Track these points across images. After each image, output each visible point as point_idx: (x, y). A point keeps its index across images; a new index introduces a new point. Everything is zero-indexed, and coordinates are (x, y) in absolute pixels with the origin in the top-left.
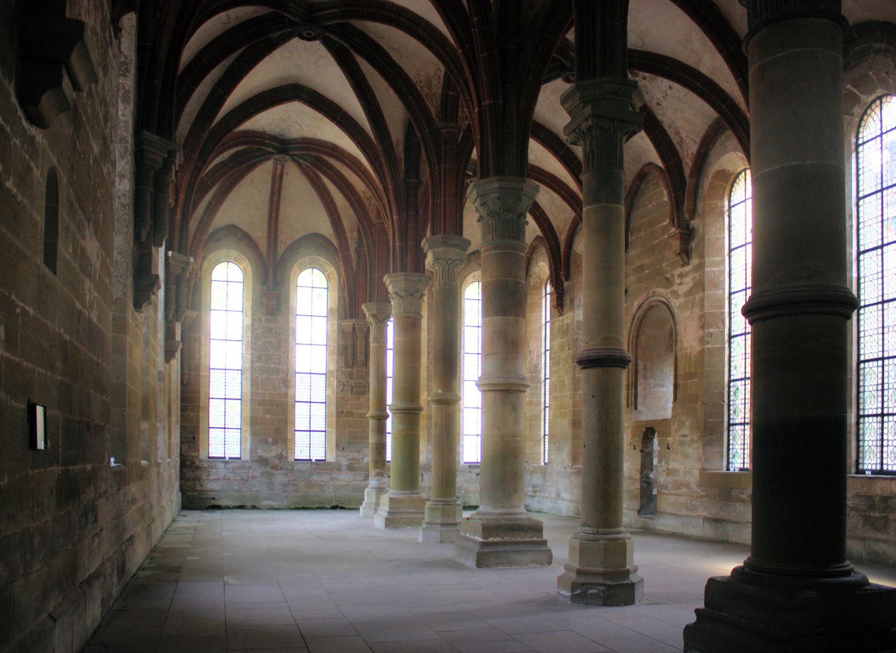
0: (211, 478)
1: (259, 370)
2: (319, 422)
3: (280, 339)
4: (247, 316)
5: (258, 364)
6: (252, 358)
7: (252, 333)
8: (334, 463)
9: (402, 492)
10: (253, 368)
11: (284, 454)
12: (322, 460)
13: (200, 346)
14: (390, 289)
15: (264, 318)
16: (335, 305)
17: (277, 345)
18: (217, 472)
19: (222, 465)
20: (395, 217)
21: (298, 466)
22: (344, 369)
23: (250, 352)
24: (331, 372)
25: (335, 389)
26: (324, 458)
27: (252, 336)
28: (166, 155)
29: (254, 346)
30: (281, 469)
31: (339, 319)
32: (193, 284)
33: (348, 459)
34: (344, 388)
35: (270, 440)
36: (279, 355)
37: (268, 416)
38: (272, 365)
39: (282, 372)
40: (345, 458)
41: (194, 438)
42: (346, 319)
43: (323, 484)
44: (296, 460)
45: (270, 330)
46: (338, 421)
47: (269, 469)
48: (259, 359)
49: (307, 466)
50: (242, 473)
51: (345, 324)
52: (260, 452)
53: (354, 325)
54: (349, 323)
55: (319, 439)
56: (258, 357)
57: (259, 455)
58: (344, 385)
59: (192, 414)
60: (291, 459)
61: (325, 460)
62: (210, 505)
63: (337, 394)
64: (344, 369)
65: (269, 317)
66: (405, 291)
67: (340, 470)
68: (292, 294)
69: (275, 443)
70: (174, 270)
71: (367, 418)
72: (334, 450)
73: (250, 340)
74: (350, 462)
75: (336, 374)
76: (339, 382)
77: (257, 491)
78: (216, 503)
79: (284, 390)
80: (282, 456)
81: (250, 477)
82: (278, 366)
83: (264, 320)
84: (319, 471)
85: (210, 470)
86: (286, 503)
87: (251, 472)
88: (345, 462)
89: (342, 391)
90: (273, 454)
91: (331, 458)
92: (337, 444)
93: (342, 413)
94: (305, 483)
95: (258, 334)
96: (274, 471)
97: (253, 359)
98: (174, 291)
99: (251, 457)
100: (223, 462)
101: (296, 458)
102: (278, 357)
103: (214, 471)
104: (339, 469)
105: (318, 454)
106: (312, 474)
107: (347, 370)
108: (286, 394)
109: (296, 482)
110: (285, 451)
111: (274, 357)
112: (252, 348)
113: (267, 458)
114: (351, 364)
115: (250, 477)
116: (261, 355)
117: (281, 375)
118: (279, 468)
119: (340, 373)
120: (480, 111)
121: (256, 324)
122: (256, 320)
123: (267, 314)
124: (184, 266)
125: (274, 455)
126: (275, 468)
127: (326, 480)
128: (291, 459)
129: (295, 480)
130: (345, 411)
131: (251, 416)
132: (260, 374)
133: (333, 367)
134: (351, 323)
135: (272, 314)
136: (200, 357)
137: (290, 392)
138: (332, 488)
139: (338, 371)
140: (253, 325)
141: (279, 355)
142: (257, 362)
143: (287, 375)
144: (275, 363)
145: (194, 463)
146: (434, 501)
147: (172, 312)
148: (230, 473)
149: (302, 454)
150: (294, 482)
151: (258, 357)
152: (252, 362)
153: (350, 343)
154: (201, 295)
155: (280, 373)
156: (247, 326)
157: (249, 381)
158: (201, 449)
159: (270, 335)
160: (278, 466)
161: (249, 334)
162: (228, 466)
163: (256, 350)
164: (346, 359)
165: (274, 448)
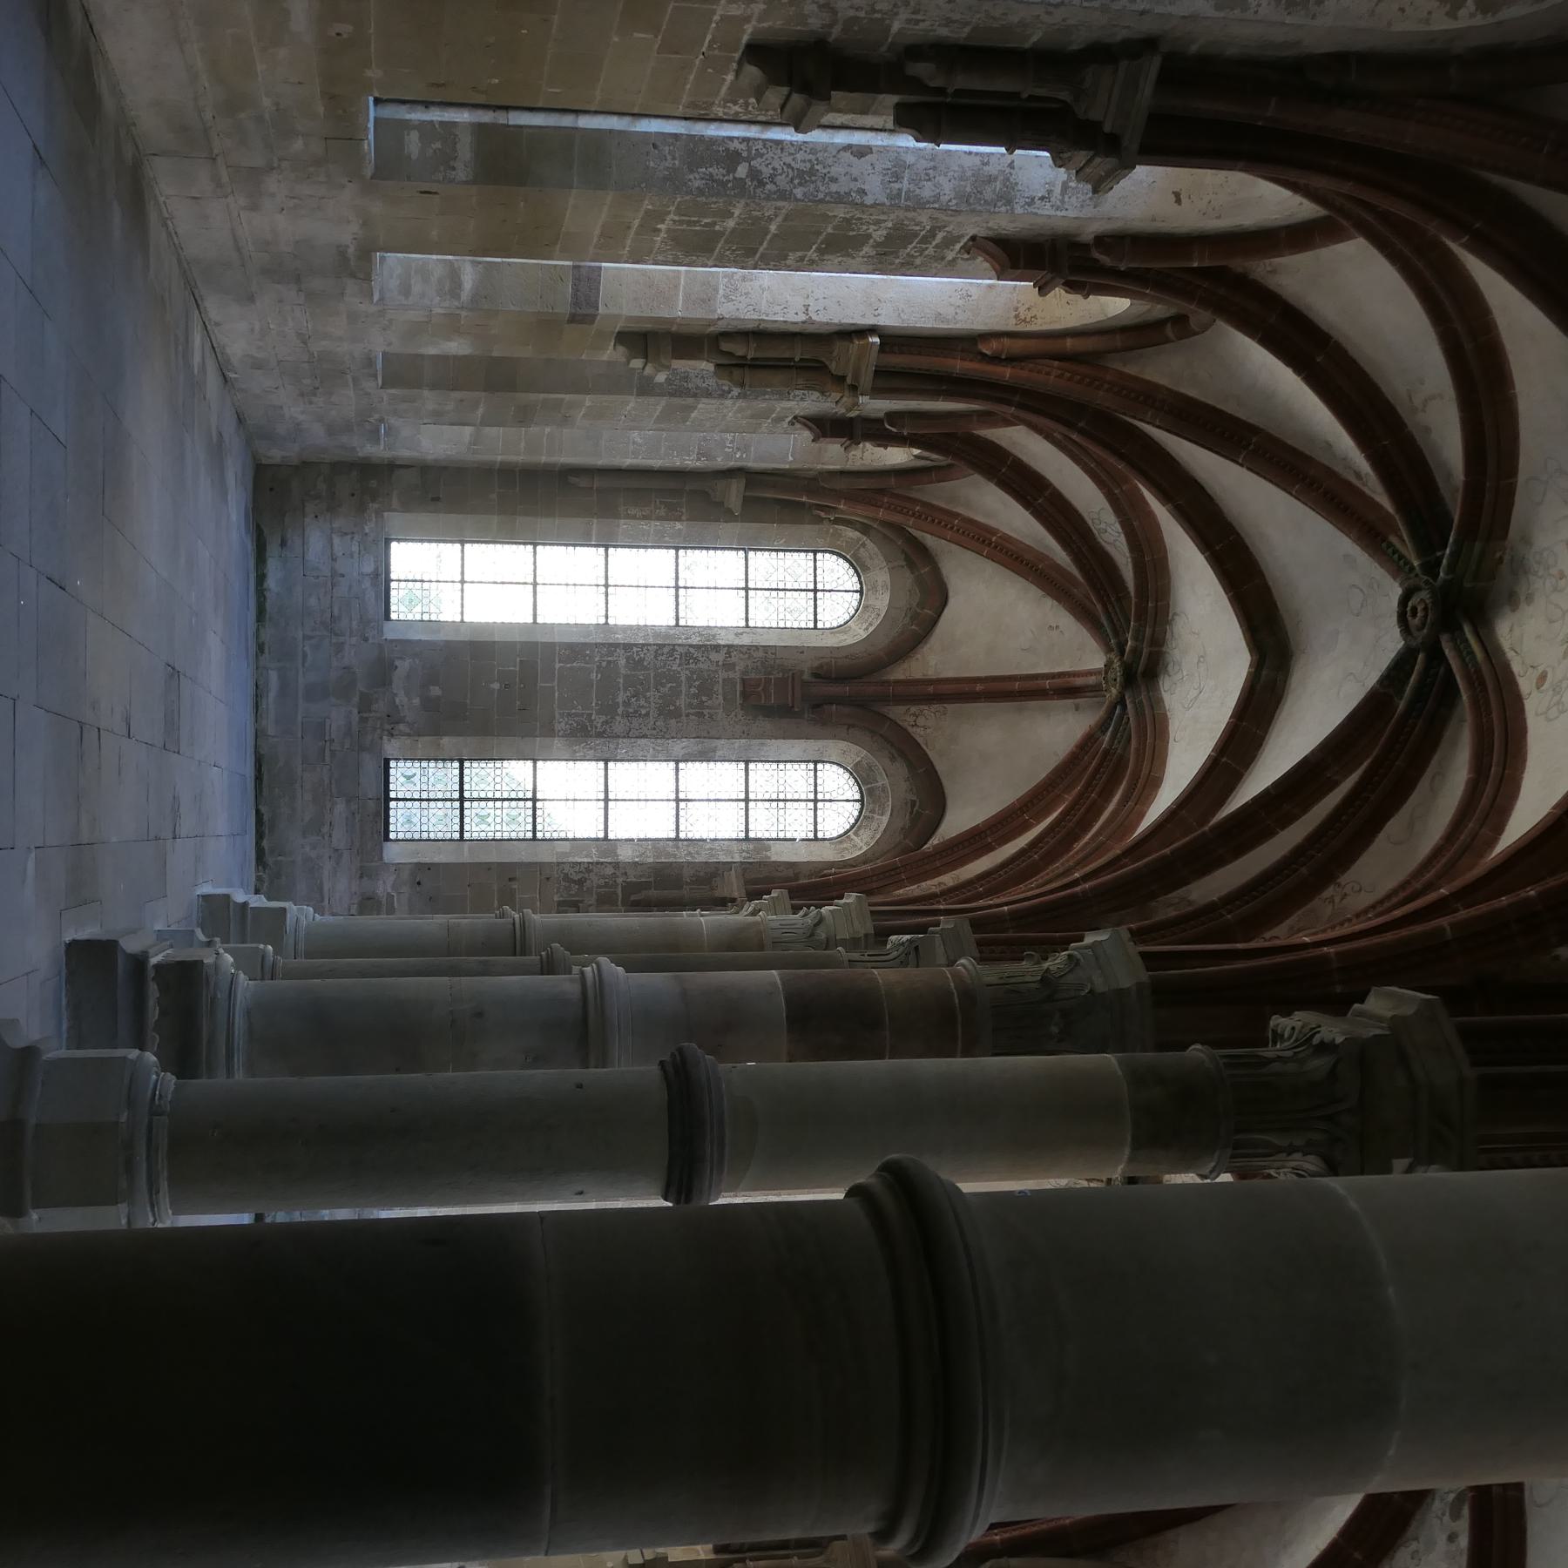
0: (336, 540)
1: (609, 662)
2: (487, 823)
3: (687, 715)
4: (737, 635)
5: (622, 662)
6: (636, 645)
7: (697, 647)
8: (381, 858)
9: (302, 934)
10: (613, 647)
11: (402, 727)
12: (387, 831)
13: (658, 518)
14: (825, 910)
15: (735, 675)
16: (779, 855)
17: (672, 708)
18: (352, 556)
19: (368, 568)
20: (1006, 908)
21: (370, 765)
22: (620, 880)
23: (651, 641)
24: (614, 852)
25: (571, 859)
26: (392, 836)
27: (691, 646)
28: (1107, 128)
29: (666, 650)
30: (363, 720)
31: (745, 867)
32: (804, 499)
33: (390, 897)
34: (574, 882)
35: (435, 691)
36: (647, 714)
37: (496, 686)
38: (621, 698)
39: (606, 722)
40: (393, 887)
41: (436, 499)
42: (746, 882)
43: (325, 829)
44: (387, 762)
45: (706, 688)
46: (488, 867)
47: (361, 687)
48: (637, 664)
49: (371, 788)
50: (351, 620)
51: (734, 879)
52: (403, 666)
53: (733, 900)
54: (734, 888)
55: (438, 822)
56: (642, 660)
57: (397, 663)
58: (581, 882)
59: (494, 496)
60: (390, 747)
61: (387, 838)
62: (266, 531)
63: (558, 864)
64: (620, 880)
65: (739, 688)
66: (827, 939)
67: (361, 877)
68: (797, 747)
69: (429, 705)
70: (835, 354)
71: (500, 906)
72: (415, 861)
73: (680, 642)
74: (384, 901)
75: (609, 860)
76: (588, 868)
77: (305, 656)
78: (273, 549)
79: (561, 725)
80: (397, 723)
81: (342, 639)
82: (620, 711)
83: (731, 675)
84: (358, 817)
85: (357, 537)
86: (271, 731)
87: (354, 640)
88: (384, 886)
89: (566, 878)
90: (401, 699)
91: (392, 853)
92: (429, 867)
93: (510, 880)
94: (327, 781)
95: (697, 661)
96: (356, 699)
97: (635, 649)
98: (787, 355)
99: (392, 641)
100: (377, 569)
101: (393, 764)
102: (643, 712)
103: (355, 548)
104: (363, 873)
105: (403, 822)
106: (348, 802)
107: (619, 891)
108: (550, 732)
109: (327, 759)
110: (408, 731)
111: (642, 702)
112: (661, 646)
113: (390, 683)
114: (633, 898)
115: (342, 639)
116: (646, 668)
117: (599, 720)
118: (365, 715)
119: (609, 871)
120: (1305, 946)
121: (718, 657)
122: (728, 653)
123: (743, 681)
124: (849, 381)
125: (397, 701)
126: (365, 704)
127: (334, 839)
128: (390, 747)
129: (333, 753)
130: (515, 886)
131: (494, 642)
132: (599, 667)
133: (625, 855)
134: (736, 895)
135: (744, 695)
136: (634, 517)
137: (558, 743)
138: (313, 854)
139: (616, 865)
140: (717, 648)
141: (647, 714)
142: (628, 658)
143: (600, 735)
144: (627, 704)
145: (373, 501)
146: (274, 965)
147: (739, 350)
148: (350, 587)
149: (402, 779)
150: (327, 753)
151: (642, 660)
152: (628, 647)
153: (686, 892)
154: (781, 522)
155: (603, 718)
156: (714, 636)
157: (582, 640)
158: (408, 516)
159: (693, 690)
160: (370, 711)
161: (695, 640)
162: (367, 584)
163: (655, 657)
164: (644, 886)
165: (416, 701)
